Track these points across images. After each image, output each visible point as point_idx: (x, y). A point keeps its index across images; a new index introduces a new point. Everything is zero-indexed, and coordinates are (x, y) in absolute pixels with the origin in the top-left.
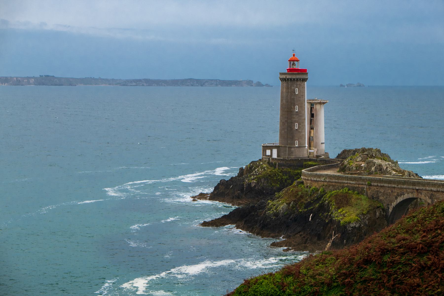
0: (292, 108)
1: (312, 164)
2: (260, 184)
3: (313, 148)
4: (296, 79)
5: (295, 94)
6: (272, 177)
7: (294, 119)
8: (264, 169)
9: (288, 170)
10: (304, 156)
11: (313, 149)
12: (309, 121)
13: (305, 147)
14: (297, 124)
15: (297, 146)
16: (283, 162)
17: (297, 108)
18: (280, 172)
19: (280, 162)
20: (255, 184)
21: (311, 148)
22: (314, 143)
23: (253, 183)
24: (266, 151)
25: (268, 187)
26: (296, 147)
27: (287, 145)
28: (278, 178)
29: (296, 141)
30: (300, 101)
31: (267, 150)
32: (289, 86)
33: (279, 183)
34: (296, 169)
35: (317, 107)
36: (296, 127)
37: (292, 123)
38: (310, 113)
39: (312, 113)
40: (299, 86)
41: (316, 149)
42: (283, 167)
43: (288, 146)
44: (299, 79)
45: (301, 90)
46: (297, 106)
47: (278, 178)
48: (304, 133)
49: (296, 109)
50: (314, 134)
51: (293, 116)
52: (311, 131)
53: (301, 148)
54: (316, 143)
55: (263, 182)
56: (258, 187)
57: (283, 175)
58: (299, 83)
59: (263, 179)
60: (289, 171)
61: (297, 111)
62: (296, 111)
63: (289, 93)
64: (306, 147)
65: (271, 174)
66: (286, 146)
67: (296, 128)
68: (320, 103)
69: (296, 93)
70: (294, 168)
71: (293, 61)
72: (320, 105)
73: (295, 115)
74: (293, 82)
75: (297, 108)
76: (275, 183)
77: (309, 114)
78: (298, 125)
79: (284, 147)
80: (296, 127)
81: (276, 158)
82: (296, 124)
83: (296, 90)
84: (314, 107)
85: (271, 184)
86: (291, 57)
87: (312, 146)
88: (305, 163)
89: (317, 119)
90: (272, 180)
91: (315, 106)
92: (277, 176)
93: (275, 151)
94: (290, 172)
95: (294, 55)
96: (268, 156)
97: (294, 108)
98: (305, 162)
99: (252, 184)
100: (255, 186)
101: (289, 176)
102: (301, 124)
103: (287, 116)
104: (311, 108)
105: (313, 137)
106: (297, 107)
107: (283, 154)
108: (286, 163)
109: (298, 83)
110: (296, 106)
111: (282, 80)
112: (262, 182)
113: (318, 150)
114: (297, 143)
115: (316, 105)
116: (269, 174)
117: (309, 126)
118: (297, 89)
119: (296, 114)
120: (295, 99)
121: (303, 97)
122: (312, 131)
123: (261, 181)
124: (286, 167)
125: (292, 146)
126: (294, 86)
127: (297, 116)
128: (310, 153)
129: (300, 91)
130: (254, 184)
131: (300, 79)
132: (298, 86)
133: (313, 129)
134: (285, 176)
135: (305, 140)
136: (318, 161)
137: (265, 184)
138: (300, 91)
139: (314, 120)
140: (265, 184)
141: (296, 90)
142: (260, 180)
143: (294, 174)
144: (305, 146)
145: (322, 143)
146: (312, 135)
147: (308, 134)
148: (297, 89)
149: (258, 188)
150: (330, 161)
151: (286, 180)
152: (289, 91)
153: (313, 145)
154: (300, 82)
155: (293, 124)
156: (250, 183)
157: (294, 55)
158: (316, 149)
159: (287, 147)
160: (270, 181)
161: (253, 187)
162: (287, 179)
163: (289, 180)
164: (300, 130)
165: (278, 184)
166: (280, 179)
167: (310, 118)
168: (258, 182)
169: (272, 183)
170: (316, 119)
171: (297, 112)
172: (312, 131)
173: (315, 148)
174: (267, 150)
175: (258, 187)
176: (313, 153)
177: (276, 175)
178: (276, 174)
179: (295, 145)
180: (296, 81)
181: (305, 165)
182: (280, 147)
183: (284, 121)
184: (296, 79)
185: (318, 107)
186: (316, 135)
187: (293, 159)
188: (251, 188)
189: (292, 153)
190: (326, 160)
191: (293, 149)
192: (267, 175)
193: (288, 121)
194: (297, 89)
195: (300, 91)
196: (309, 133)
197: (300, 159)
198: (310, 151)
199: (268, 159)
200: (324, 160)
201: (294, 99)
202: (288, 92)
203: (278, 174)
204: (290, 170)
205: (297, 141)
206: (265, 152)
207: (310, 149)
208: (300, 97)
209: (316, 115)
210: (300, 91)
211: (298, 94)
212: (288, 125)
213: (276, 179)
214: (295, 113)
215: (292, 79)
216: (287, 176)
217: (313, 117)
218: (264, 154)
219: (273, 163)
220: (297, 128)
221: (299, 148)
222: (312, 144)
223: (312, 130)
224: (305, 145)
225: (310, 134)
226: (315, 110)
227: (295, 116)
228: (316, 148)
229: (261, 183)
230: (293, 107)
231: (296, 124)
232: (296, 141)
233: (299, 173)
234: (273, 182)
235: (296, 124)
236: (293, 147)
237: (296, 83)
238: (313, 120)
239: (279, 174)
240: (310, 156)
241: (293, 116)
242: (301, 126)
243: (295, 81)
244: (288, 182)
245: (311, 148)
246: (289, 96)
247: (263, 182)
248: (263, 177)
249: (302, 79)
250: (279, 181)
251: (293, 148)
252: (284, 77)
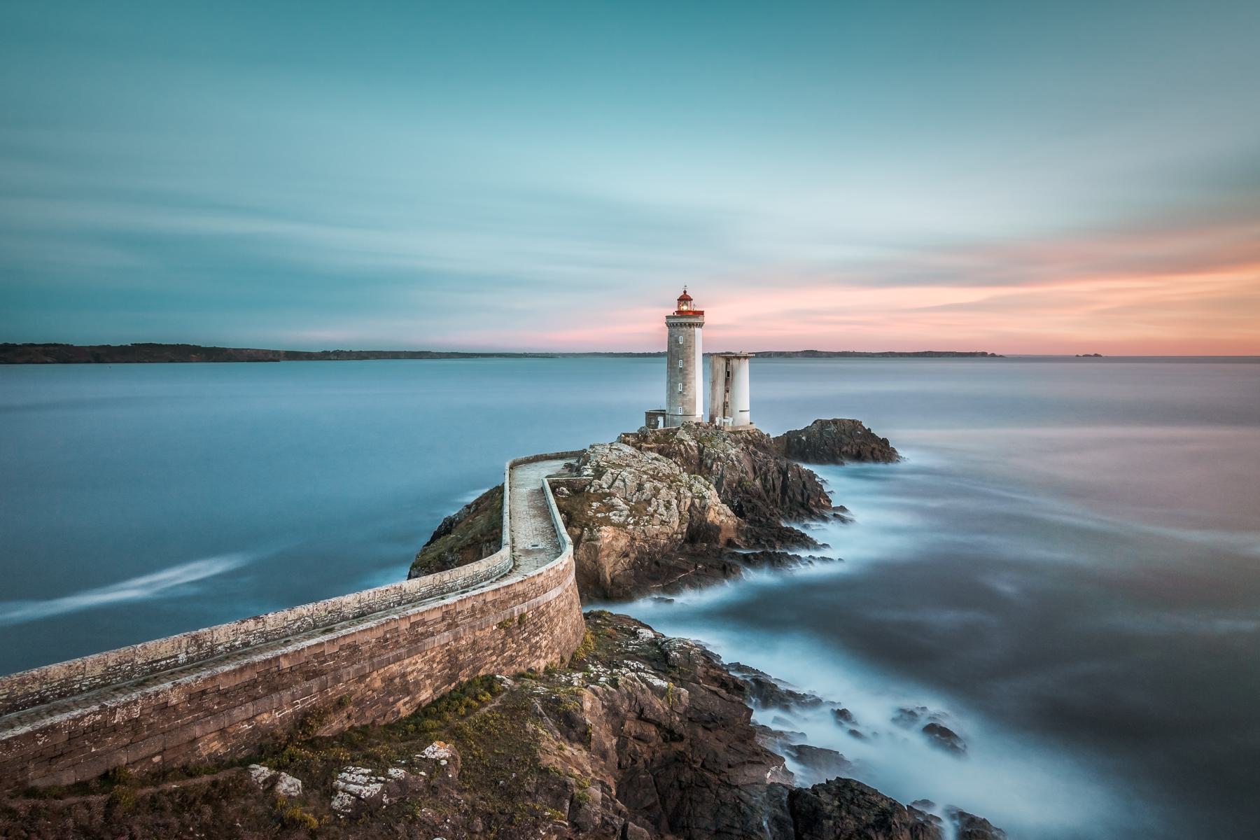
41: (731, 419)
58: (685, 329)
68: (739, 358)
71: (685, 299)
93: (661, 419)
95: (685, 292)
105: (727, 403)
111: (670, 325)
122: (727, 394)
145: (741, 411)
157: (685, 292)
164: (685, 393)
172: (727, 394)
185: (735, 362)
198: (725, 420)
207: (724, 418)
222: (727, 410)
228: (731, 417)
252: (672, 321)
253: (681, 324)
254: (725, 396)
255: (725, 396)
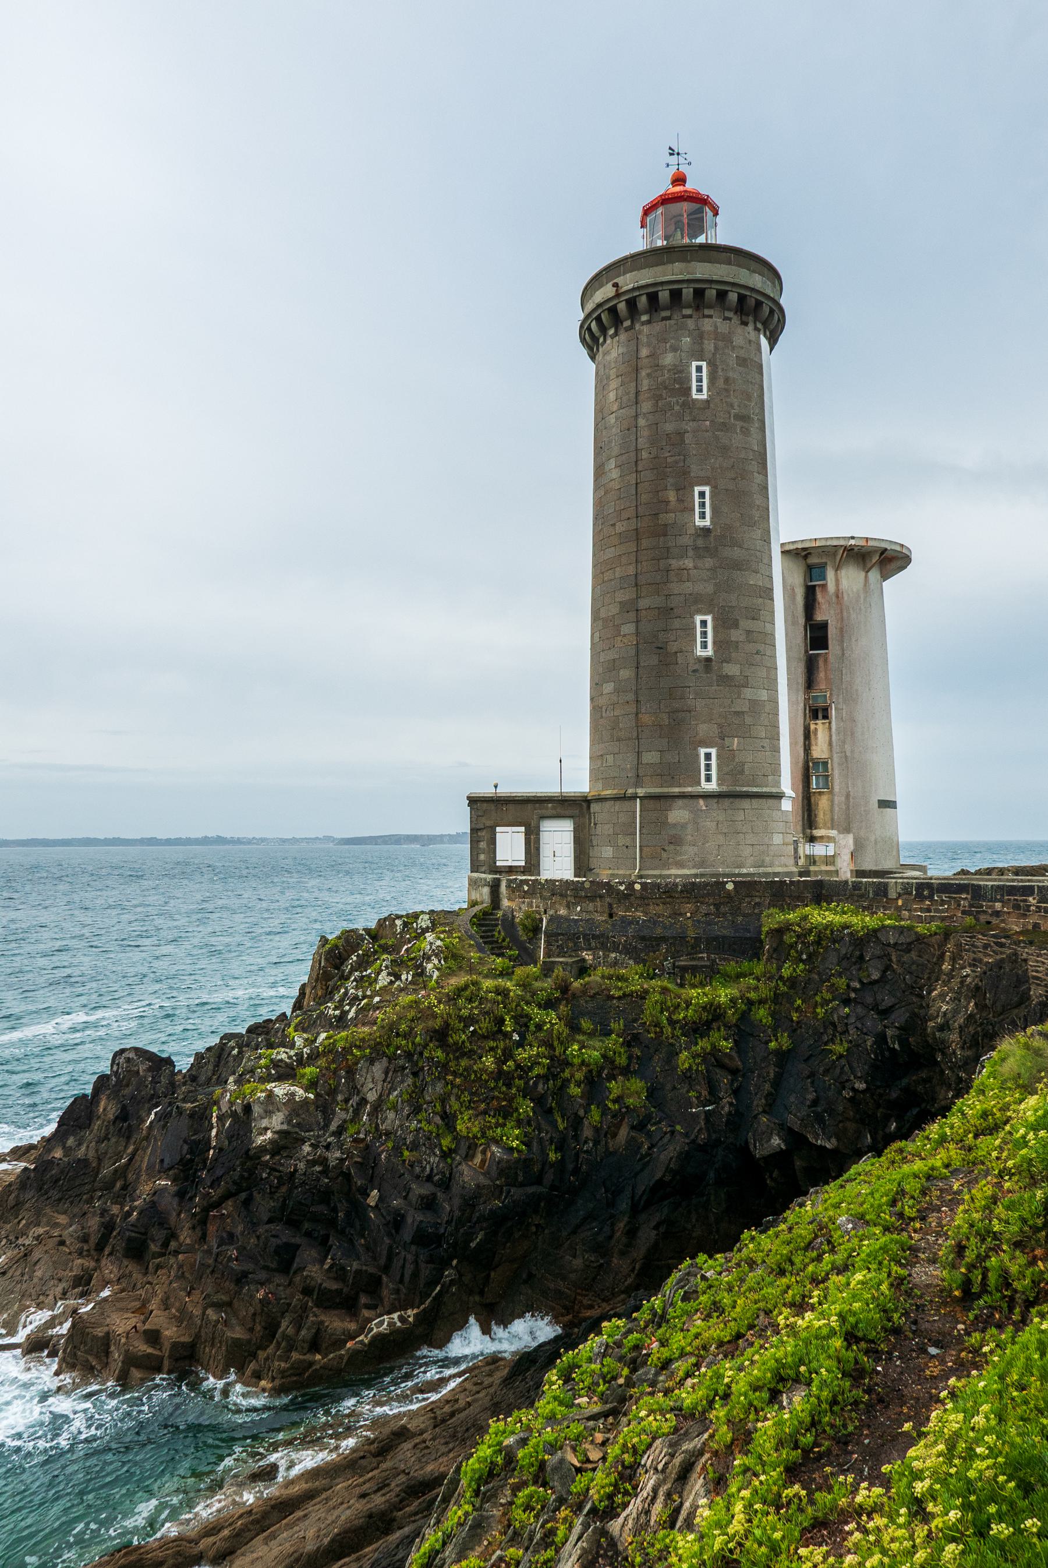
0: (667, 502)
1: (846, 926)
2: (340, 1115)
3: (833, 833)
4: (688, 293)
5: (689, 405)
6: (460, 1051)
7: (688, 587)
8: (420, 973)
9: (620, 978)
10: (770, 870)
11: (830, 839)
12: (800, 669)
13: (779, 796)
14: (709, 618)
15: (713, 786)
16: (591, 906)
17: (702, 505)
18: (549, 1004)
19: (563, 912)
20: (288, 1120)
21: (817, 833)
22: (836, 799)
23: (268, 1113)
24: (494, 833)
25: (414, 1147)
26: (707, 796)
27: (638, 781)
28: (522, 1055)
29: (703, 751)
30: (725, 449)
31: (498, 829)
32: (644, 352)
33: (526, 1107)
34: (694, 970)
35: (845, 584)
36: (704, 645)
37: (666, 612)
38: (802, 621)
39: (819, 617)
40: (716, 348)
42: (587, 956)
43: (641, 792)
44: (711, 294)
45: (731, 374)
46: (707, 489)
47: (522, 1055)
48: (764, 695)
49: (697, 510)
50: (830, 744)
51: (674, 563)
52: (812, 727)
53: (746, 803)
54: (848, 796)
55: (372, 1097)
56: (328, 1147)
57: (574, 1028)
58: (713, 323)
59: (378, 1069)
60: (631, 995)
61: (707, 522)
62: (698, 522)
63: (641, 397)
64: (786, 805)
65: (461, 1018)
66: (630, 791)
67: (700, 652)
69: (695, 395)
70: (683, 962)
72: (863, 574)
73: (691, 553)
74: (669, 318)
75: (702, 505)
76: (485, 1112)
77: (794, 623)
78: (715, 628)
79: (616, 799)
80: (704, 645)
81: (567, 883)
82: (698, 618)
83: (694, 374)
84: (824, 587)
85: (449, 1120)
86: (663, 186)
87: (821, 816)
88: (773, 918)
89: (847, 653)
90: (455, 1074)
91: (830, 574)
92: (507, 1036)
94: (644, 995)
95: (679, 179)
96: (511, 870)
97: (680, 501)
98: (772, 910)
99: (264, 1123)
100: (286, 1143)
101: (632, 1041)
102: (736, 625)
103: (631, 570)
104: (810, 593)
106: (702, 494)
107: (608, 852)
108: (611, 916)
109: (707, 325)
110: (697, 489)
112: (363, 1101)
113: (859, 847)
114: (708, 767)
115: (837, 569)
116: (438, 1023)
117: (801, 697)
118: (699, 369)
119: (696, 548)
120: (688, 438)
121: (746, 432)
122: (819, 727)
123: (354, 1089)
124: (615, 949)
125: (676, 790)
126: (674, 349)
127: (709, 562)
128: (812, 860)
129: (727, 380)
130: (277, 1121)
131: (722, 295)
132: (709, 346)
133: (826, 717)
134: (591, 1035)
135: (776, 750)
136: (893, 895)
137: (391, 1115)
138: (720, 383)
139: (831, 658)
140: (390, 1119)
141: (694, 374)
142: (351, 1072)
143: (671, 1022)
144: (774, 790)
146: (819, 751)
147: (793, 744)
148: (699, 369)
149: (323, 1161)
150: (1028, 891)
151: (594, 1083)
152: (645, 384)
153: (832, 810)
154: (726, 319)
155: (677, 623)
156: (248, 1108)
157: (679, 179)
158: (848, 842)
159: (634, 797)
160: (434, 1090)
161: (262, 1149)
162: (610, 1068)
163: (626, 1072)
164: (732, 669)
165: (519, 1124)
166: (536, 1071)
167: (806, 652)
168: (333, 1092)
169: (454, 1105)
170: (843, 654)
171: (706, 531)
173: (840, 832)
174: (498, 829)
175: (328, 1147)
176: (830, 860)
177: (498, 1032)
178: (502, 1021)
179: (699, 783)
180: (689, 307)
181: (779, 932)
182: (595, 807)
183: (614, 609)
184: (688, 293)
186: (848, 747)
187: (676, 885)
188: (251, 1157)
189: (676, 841)
190: (976, 892)
191: (678, 814)
192: (418, 1029)
193: (643, 603)
194: (704, 364)
195: (720, 383)
196: (801, 739)
197: (730, 886)
199: (486, 890)
200: (962, 888)
201: (681, 434)
202: (637, 393)
203: (522, 1021)
204: (636, 985)
205: (713, 751)
206: (483, 845)
207: (812, 839)
208: (725, 427)
209: (841, 630)
210: (727, 380)
211: (707, 401)
212: (637, 634)
213: (499, 1074)
214: (686, 540)
215: (664, 296)
216: (608, 1033)
217: (827, 648)
218: (482, 857)
219: (519, 916)
220: (709, 652)
221: (727, 802)
222: (823, 804)
223: (819, 722)
224: (778, 784)
225: (807, 749)
226: (834, 599)
227: (689, 563)
228: (847, 830)
229: (357, 1112)
230: (672, 496)
231: (704, 623)
232: (703, 751)
233: (719, 1006)
234: (466, 1097)
235: (704, 623)
236: (683, 796)
237: (690, 323)
238: (826, 661)
239: (537, 1013)
240: (812, 868)
241: (674, 563)
242: (736, 635)
243: (688, 312)
244: (617, 1100)
245: (817, 833)
246: (642, 422)
247: (372, 1097)
248: (377, 1051)
249: (733, 297)
250: (526, 1092)
251: (680, 802)
253: (699, 293)
254: (807, 735)
255: (807, 735)
